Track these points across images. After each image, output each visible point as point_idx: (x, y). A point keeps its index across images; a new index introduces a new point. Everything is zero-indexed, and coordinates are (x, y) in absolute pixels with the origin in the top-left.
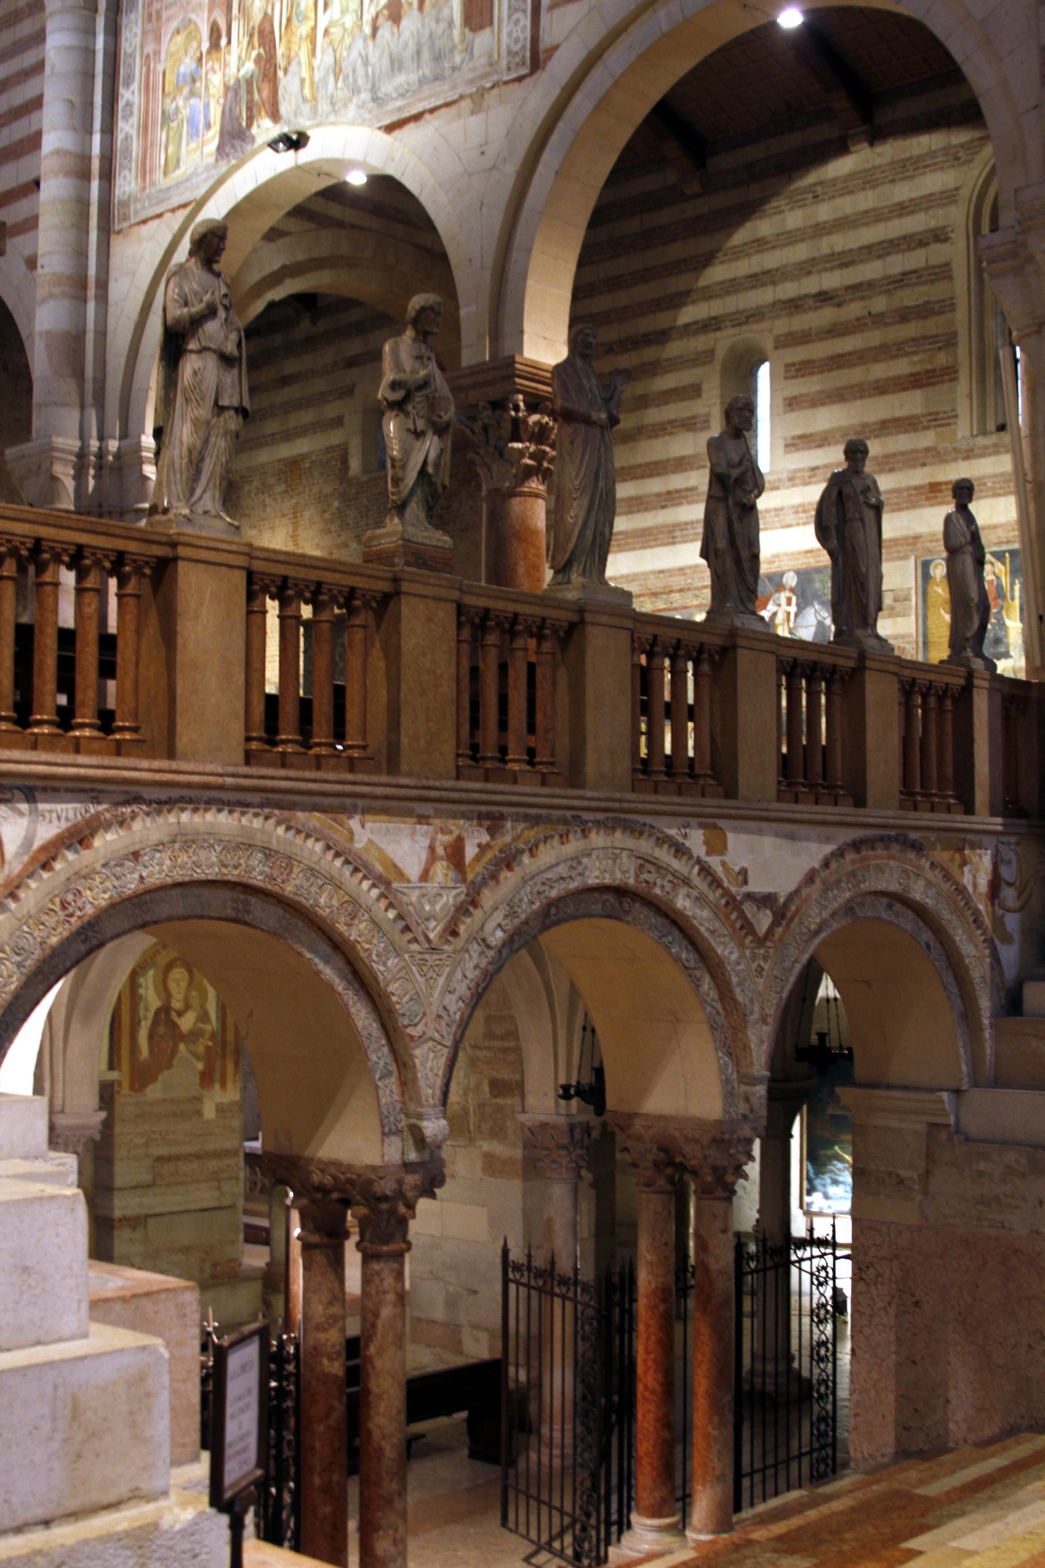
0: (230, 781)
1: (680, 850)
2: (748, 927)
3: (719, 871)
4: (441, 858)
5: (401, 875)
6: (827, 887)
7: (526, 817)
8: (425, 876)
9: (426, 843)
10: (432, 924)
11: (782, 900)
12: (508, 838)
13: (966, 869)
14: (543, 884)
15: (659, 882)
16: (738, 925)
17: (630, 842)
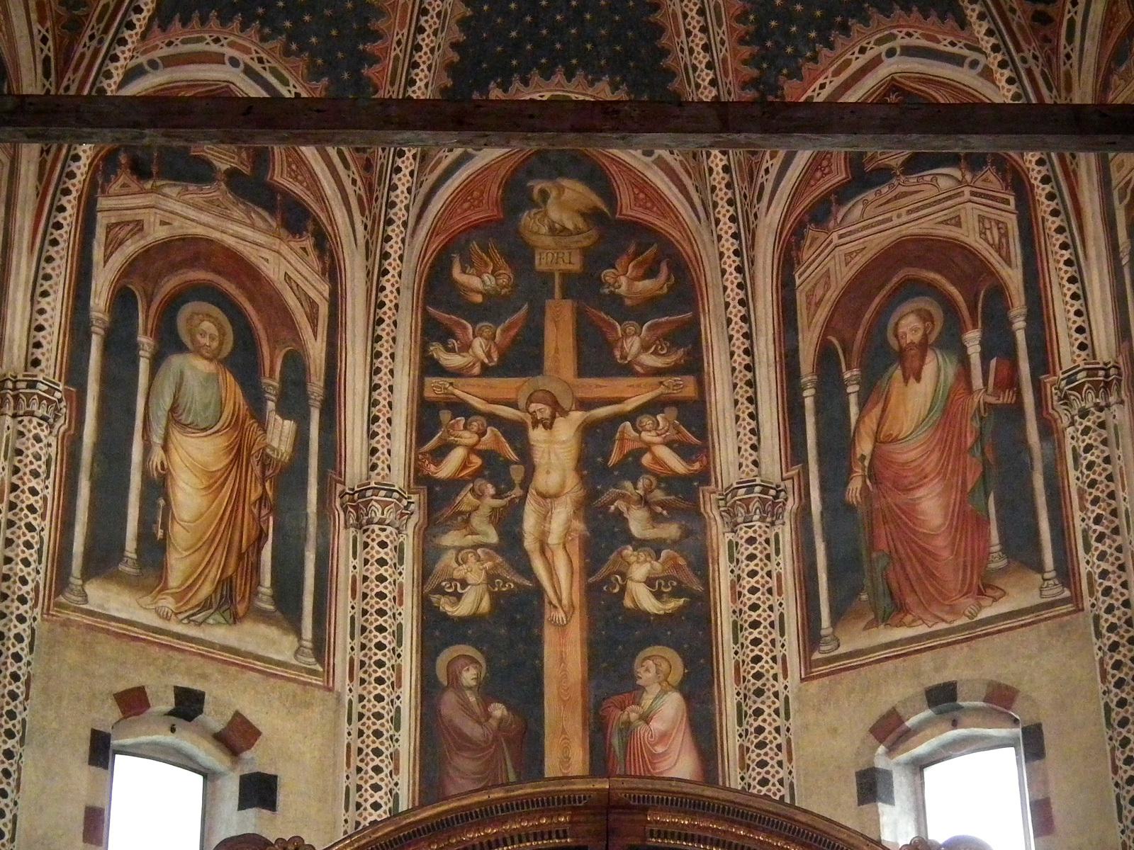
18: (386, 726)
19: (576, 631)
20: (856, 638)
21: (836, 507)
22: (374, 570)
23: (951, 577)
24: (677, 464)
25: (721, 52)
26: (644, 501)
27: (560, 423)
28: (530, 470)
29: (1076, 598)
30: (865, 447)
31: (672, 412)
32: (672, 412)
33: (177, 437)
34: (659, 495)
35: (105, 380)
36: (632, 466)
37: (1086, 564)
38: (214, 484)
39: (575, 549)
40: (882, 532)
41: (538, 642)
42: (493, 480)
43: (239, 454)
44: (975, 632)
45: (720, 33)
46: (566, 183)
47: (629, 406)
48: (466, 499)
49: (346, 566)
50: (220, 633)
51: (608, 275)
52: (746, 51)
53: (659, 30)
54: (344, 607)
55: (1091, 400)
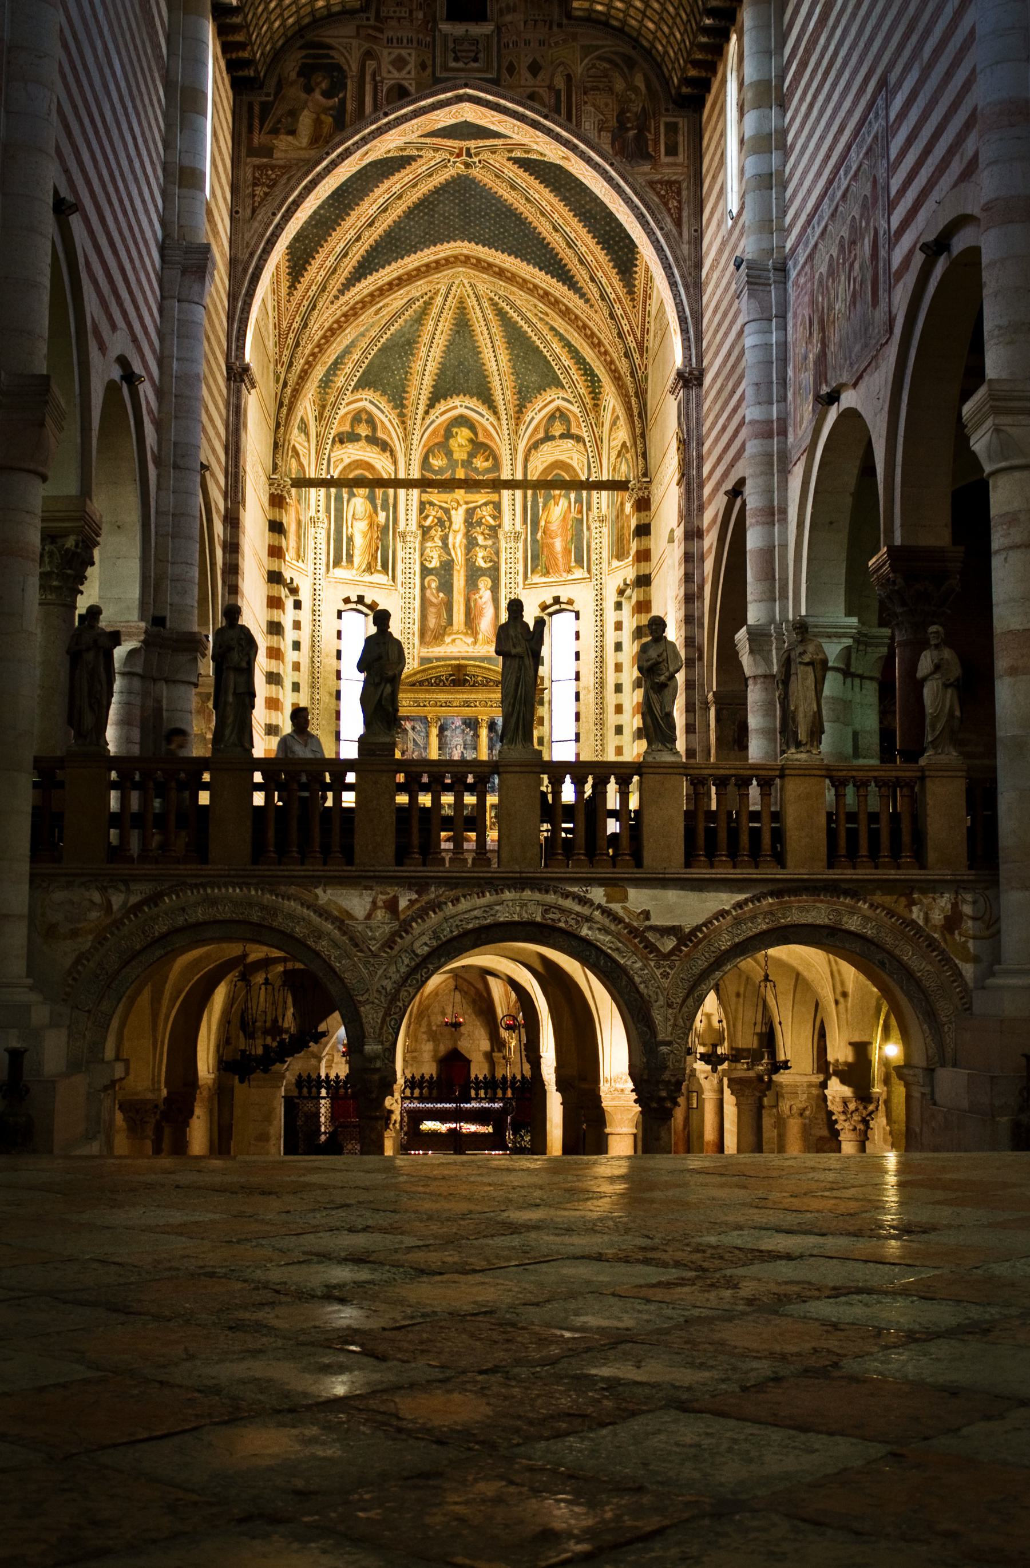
0: (232, 872)
1: (583, 901)
2: (651, 947)
3: (621, 913)
4: (381, 908)
5: (351, 917)
6: (738, 921)
7: (447, 884)
8: (369, 917)
9: (371, 900)
10: (374, 942)
11: (687, 930)
12: (433, 896)
13: (915, 909)
14: (461, 921)
15: (563, 919)
16: (641, 946)
17: (537, 896)
18: (411, 611)
19: (462, 573)
20: (536, 579)
21: (534, 541)
22: (408, 556)
23: (562, 568)
24: (492, 522)
25: (509, 398)
26: (483, 533)
27: (460, 509)
28: (451, 523)
29: (590, 578)
30: (542, 523)
31: (491, 506)
32: (491, 506)
33: (355, 522)
34: (487, 532)
35: (336, 510)
36: (479, 523)
37: (594, 568)
38: (365, 536)
39: (463, 548)
40: (545, 549)
41: (452, 575)
42: (441, 526)
43: (371, 525)
44: (567, 582)
45: (508, 392)
46: (463, 429)
47: (479, 504)
48: (433, 532)
49: (400, 554)
50: (367, 578)
51: (474, 460)
52: (516, 397)
53: (490, 389)
54: (400, 566)
55: (598, 524)
